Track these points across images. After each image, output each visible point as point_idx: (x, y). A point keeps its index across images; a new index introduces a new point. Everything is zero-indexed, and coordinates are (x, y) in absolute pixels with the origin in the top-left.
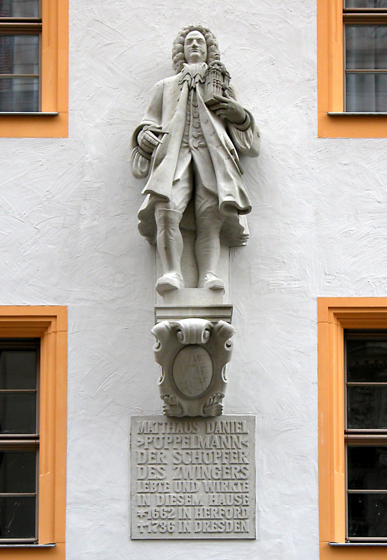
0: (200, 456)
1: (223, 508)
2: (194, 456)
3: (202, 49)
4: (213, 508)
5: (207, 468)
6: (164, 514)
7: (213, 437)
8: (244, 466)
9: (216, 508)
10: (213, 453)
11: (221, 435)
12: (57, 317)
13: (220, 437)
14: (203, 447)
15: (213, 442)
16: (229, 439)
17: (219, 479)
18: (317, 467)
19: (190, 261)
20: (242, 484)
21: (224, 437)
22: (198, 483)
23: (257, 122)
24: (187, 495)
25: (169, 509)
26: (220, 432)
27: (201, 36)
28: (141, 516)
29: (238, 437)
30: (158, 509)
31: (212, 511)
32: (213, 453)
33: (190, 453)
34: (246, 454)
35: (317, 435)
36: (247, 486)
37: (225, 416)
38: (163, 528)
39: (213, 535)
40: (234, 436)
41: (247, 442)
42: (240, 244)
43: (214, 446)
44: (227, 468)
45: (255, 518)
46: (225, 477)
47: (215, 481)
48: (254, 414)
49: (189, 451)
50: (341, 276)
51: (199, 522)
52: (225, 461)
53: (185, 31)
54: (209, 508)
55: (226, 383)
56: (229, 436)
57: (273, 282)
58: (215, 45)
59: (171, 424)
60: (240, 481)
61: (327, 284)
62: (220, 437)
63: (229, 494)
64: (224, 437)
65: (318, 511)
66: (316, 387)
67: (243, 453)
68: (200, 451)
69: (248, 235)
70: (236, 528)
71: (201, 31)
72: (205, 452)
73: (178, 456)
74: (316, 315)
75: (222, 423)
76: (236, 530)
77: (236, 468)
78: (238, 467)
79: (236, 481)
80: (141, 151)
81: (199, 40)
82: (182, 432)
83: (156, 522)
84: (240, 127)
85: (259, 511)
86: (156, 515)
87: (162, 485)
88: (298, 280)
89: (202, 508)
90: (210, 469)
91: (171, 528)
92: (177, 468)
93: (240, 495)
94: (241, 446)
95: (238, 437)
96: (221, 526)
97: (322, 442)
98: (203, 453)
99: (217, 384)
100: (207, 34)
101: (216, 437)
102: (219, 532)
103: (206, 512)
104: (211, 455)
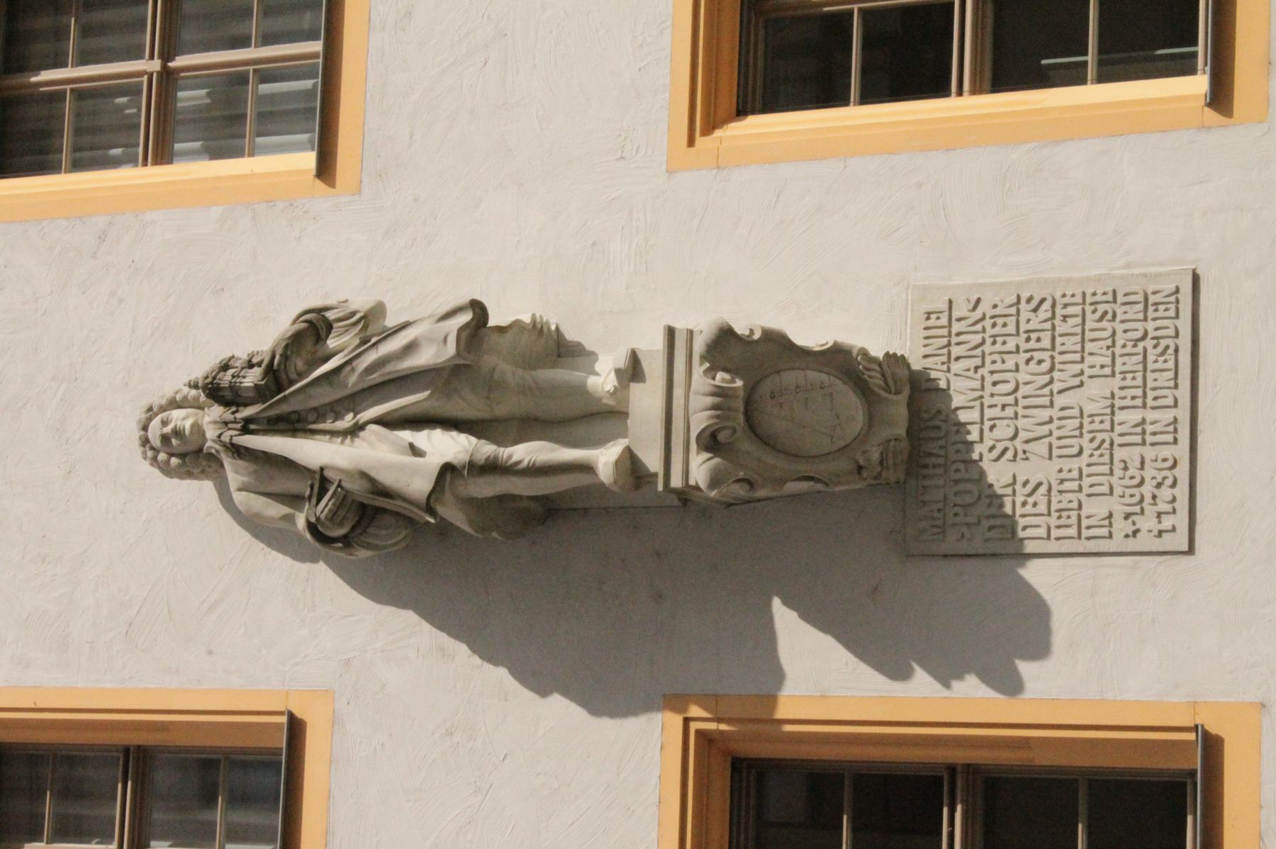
0: (999, 400)
1: (1119, 342)
2: (996, 412)
4: (1118, 368)
5: (1026, 384)
6: (1132, 478)
7: (956, 375)
8: (1023, 301)
9: (1119, 361)
10: (992, 372)
11: (953, 357)
13: (957, 359)
14: (978, 393)
15: (967, 374)
16: (962, 338)
17: (1052, 357)
19: (580, 430)
20: (1066, 306)
22: (1060, 401)
23: (316, 303)
24: (1087, 427)
25: (1118, 466)
26: (945, 359)
27: (156, 422)
28: (1134, 528)
29: (959, 320)
30: (1118, 490)
32: (992, 372)
33: (992, 423)
34: (996, 300)
38: (1164, 478)
39: (1181, 365)
40: (957, 327)
43: (976, 372)
44: (1028, 340)
45: (1145, 275)
46: (1046, 343)
47: (1058, 366)
48: (908, 288)
49: (987, 424)
51: (1150, 394)
52: (1011, 346)
53: (150, 453)
54: (1119, 376)
56: (954, 340)
59: (926, 466)
60: (1059, 312)
62: (957, 359)
63: (1087, 333)
64: (956, 351)
67: (995, 306)
68: (987, 401)
69: (534, 315)
71: (150, 419)
72: (989, 388)
73: (1000, 447)
75: (925, 357)
76: (1172, 313)
77: (1028, 321)
79: (1058, 317)
80: (358, 531)
81: (165, 423)
82: (941, 443)
84: (323, 333)
85: (1128, 266)
86: (1132, 496)
87: (1062, 481)
90: (1029, 378)
92: (1024, 452)
93: (1089, 309)
94: (977, 314)
95: (959, 320)
96: (1160, 349)
98: (992, 395)
99: (839, 360)
100: (155, 409)
101: (956, 367)
102: (1176, 351)
103: (1128, 383)
104: (996, 377)
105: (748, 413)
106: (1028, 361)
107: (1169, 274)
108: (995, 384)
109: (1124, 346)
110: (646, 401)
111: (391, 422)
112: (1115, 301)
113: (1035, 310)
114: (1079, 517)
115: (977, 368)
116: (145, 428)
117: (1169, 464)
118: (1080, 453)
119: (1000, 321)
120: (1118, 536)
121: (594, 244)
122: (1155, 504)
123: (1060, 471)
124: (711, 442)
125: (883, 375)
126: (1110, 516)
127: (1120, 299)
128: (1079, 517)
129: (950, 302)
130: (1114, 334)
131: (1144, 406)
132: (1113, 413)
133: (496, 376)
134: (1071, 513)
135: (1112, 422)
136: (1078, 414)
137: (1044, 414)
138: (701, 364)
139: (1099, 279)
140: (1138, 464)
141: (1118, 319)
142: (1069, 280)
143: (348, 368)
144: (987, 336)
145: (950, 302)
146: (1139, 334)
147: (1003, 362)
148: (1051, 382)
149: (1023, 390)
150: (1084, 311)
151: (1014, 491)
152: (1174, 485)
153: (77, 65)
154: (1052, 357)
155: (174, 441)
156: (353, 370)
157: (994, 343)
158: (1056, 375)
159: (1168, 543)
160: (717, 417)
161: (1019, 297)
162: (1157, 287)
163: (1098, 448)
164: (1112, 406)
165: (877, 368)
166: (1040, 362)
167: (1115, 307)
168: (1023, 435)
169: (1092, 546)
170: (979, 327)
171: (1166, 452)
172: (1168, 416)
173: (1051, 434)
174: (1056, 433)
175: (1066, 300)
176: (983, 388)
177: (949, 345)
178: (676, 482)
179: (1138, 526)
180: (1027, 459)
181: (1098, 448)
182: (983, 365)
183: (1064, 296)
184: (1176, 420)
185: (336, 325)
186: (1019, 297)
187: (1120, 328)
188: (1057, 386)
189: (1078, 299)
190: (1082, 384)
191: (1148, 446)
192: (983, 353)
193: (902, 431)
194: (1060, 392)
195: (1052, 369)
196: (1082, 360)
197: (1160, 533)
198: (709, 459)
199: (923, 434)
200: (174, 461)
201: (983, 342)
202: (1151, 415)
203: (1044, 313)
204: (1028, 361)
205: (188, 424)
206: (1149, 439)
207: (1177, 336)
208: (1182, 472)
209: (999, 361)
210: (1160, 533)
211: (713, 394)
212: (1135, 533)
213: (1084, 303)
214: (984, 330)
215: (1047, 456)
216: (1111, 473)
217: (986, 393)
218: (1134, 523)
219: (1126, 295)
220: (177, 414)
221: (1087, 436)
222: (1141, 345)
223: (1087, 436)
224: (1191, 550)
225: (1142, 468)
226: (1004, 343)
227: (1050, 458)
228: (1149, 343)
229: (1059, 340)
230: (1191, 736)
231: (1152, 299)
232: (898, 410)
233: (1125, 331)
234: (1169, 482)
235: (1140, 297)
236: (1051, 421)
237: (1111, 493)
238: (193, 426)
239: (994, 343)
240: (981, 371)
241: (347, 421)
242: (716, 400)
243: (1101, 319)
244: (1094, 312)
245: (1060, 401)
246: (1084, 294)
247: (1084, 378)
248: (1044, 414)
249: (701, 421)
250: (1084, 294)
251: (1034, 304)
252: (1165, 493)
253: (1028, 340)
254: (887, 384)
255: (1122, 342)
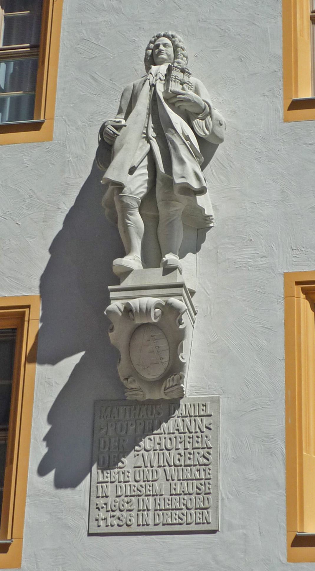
1: (186, 497)
2: (158, 440)
3: (168, 52)
4: (173, 497)
8: (209, 450)
9: (178, 497)
10: (176, 437)
11: (184, 418)
12: (31, 307)
13: (183, 421)
17: (181, 466)
18: (284, 449)
20: (204, 470)
21: (187, 420)
22: (160, 470)
26: (184, 414)
28: (100, 508)
30: (118, 499)
31: (174, 501)
32: (176, 437)
34: (210, 437)
35: (284, 414)
36: (211, 472)
37: (189, 398)
38: (122, 521)
40: (198, 419)
41: (210, 424)
42: (207, 226)
43: (176, 430)
44: (190, 454)
45: (217, 507)
46: (188, 462)
47: (176, 468)
48: (219, 394)
50: (308, 250)
51: (161, 513)
52: (188, 446)
53: (153, 39)
55: (184, 363)
56: (193, 418)
57: (240, 260)
58: (181, 48)
61: (294, 259)
62: (183, 421)
63: (191, 481)
64: (187, 420)
65: (285, 497)
66: (283, 363)
67: (207, 437)
70: (198, 519)
74: (282, 290)
75: (185, 405)
76: (198, 521)
77: (199, 453)
78: (202, 452)
81: (165, 45)
82: (145, 417)
83: (114, 513)
85: (222, 499)
86: (115, 506)
87: (123, 473)
88: (265, 257)
89: (163, 497)
91: (130, 520)
97: (290, 421)
101: (180, 420)
102: (180, 524)
105: (143, 325)
106: (180, 454)
107: (217, 518)
108: (170, 439)
109: (184, 499)
110: (155, 276)
111: (151, 154)
112: (206, 494)
113: (204, 456)
114: (107, 482)
115: (178, 430)
116: (164, 36)
117: (129, 523)
118: (136, 481)
119: (200, 440)
120: (98, 501)
121: (251, 240)
122: (111, 517)
123: (128, 472)
124: (128, 310)
125: (172, 387)
126: (107, 497)
127: (206, 496)
128: (107, 482)
129: (210, 416)
130: (190, 494)
131: (156, 510)
132: (153, 495)
133: (174, 202)
134: (109, 478)
135: (150, 495)
136: (206, 477)
137: (155, 464)
138: (164, 301)
139: (217, 486)
140: (130, 508)
141: (196, 496)
142: (218, 472)
143: (174, 132)
144: (193, 434)
145: (210, 416)
146: (189, 506)
147: (180, 443)
148: (170, 466)
149: (167, 453)
150: (202, 479)
151: (204, 448)
152: (119, 525)
153: (5, 18)
154: (181, 466)
155: (157, 50)
156: (173, 134)
157: (190, 438)
158: (173, 468)
159: (94, 523)
160: (136, 311)
161: (210, 448)
162: (210, 513)
163: (138, 489)
164: (157, 495)
165: (174, 384)
166: (179, 460)
167: (203, 494)
168: (146, 454)
169: (94, 489)
170: (198, 430)
171: (134, 520)
172: (150, 522)
173: (146, 467)
174: (146, 469)
175: (208, 471)
176: (169, 434)
177: (191, 416)
178: (112, 295)
179: (101, 509)
180: (135, 456)
181: (138, 489)
182: (180, 433)
183: (209, 470)
184: (148, 525)
185: (204, 121)
186: (210, 448)
187: (193, 497)
188: (167, 468)
189: (208, 476)
190: (168, 480)
191: (137, 512)
192: (185, 433)
193: (148, 397)
194: (164, 470)
195: (175, 466)
196: (179, 480)
197: (97, 520)
198: (120, 310)
199: (150, 407)
200: (150, 51)
201: (190, 433)
202: (151, 513)
203: (202, 460)
204: (180, 454)
205: (164, 56)
206: (140, 513)
207: (187, 524)
208: (125, 529)
209: (182, 440)
210: (97, 520)
211: (147, 309)
212: (98, 508)
213: (206, 479)
214: (196, 432)
215: (136, 466)
216: (126, 496)
217: (167, 436)
218: (102, 508)
219: (208, 499)
220: (170, 50)
221: (143, 484)
222: (184, 507)
223: (143, 484)
224: (89, 535)
225: (127, 510)
226: (189, 443)
227: (135, 467)
228: (185, 511)
229: (189, 468)
230: (9, 537)
231: (205, 511)
232: (157, 395)
233: (191, 499)
234: (121, 523)
235: (207, 505)
236: (152, 467)
237: (117, 497)
238: (163, 58)
239: (190, 438)
240: (177, 432)
241: (152, 134)
242: (144, 310)
243: (197, 488)
244: (201, 484)
245: (160, 470)
246: (210, 479)
247: (171, 481)
248: (155, 464)
249: (135, 303)
250: (210, 479)
251: (207, 455)
252: (115, 522)
253: (190, 454)
254: (168, 388)
255: (186, 498)
